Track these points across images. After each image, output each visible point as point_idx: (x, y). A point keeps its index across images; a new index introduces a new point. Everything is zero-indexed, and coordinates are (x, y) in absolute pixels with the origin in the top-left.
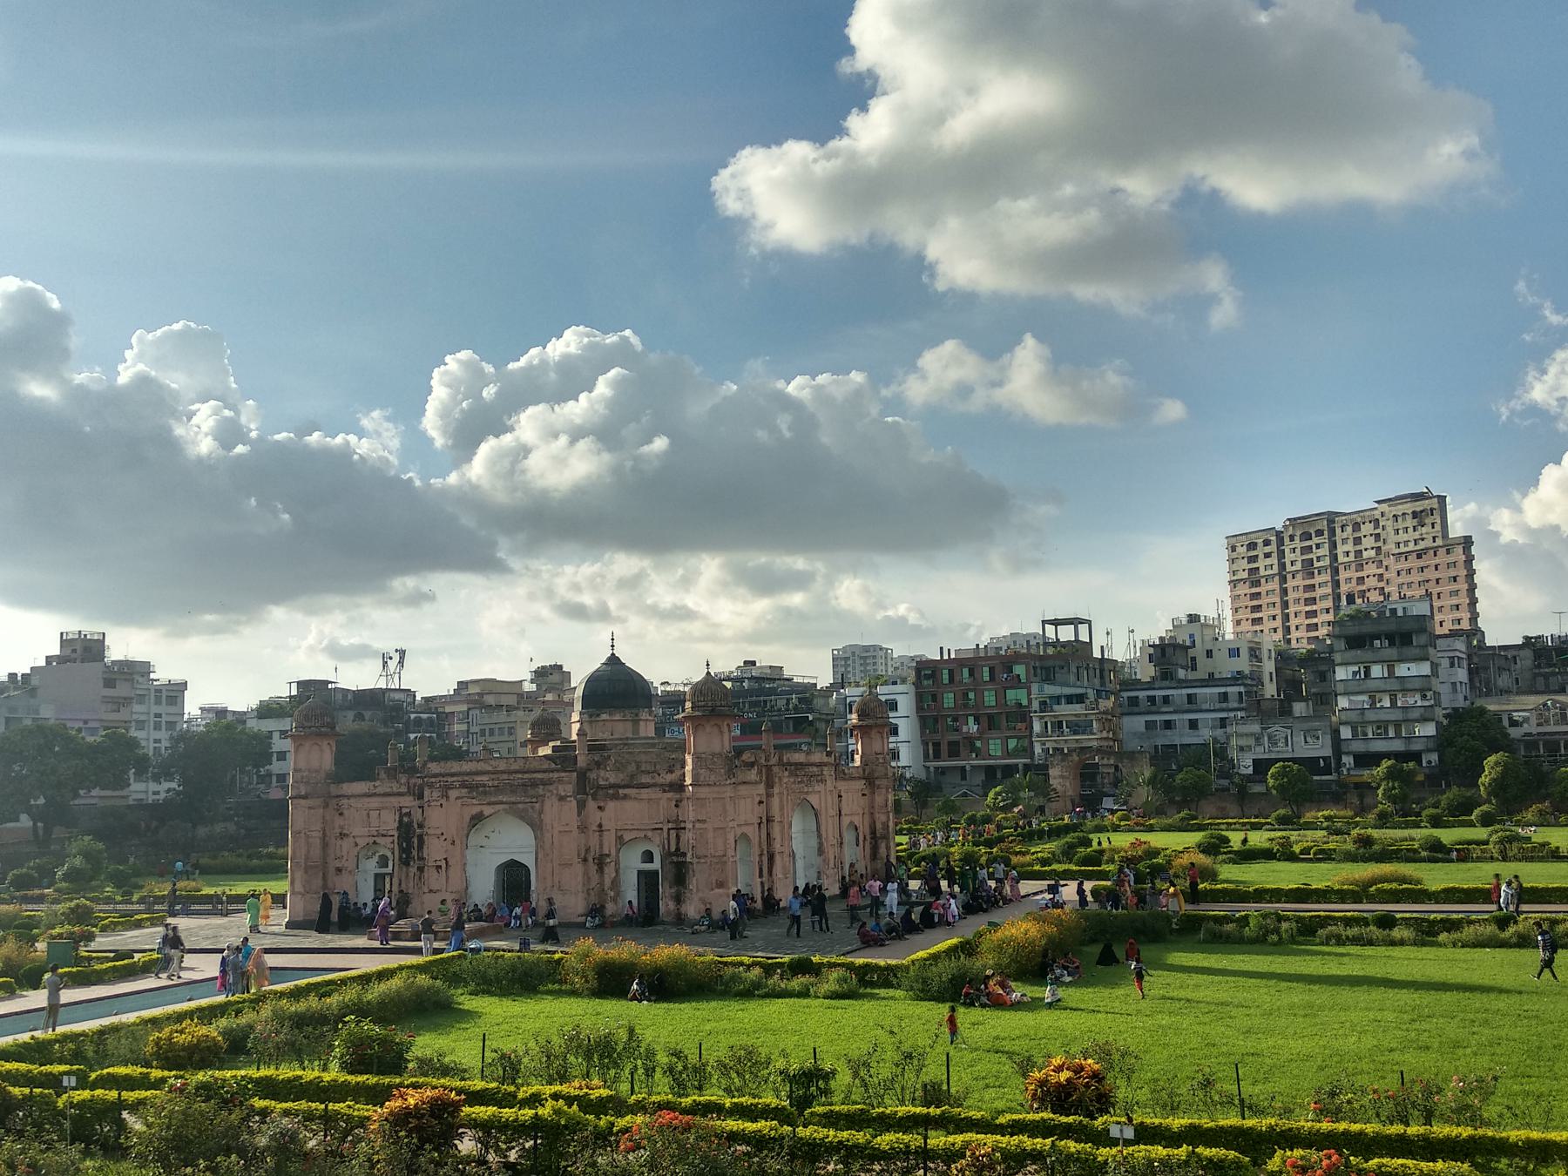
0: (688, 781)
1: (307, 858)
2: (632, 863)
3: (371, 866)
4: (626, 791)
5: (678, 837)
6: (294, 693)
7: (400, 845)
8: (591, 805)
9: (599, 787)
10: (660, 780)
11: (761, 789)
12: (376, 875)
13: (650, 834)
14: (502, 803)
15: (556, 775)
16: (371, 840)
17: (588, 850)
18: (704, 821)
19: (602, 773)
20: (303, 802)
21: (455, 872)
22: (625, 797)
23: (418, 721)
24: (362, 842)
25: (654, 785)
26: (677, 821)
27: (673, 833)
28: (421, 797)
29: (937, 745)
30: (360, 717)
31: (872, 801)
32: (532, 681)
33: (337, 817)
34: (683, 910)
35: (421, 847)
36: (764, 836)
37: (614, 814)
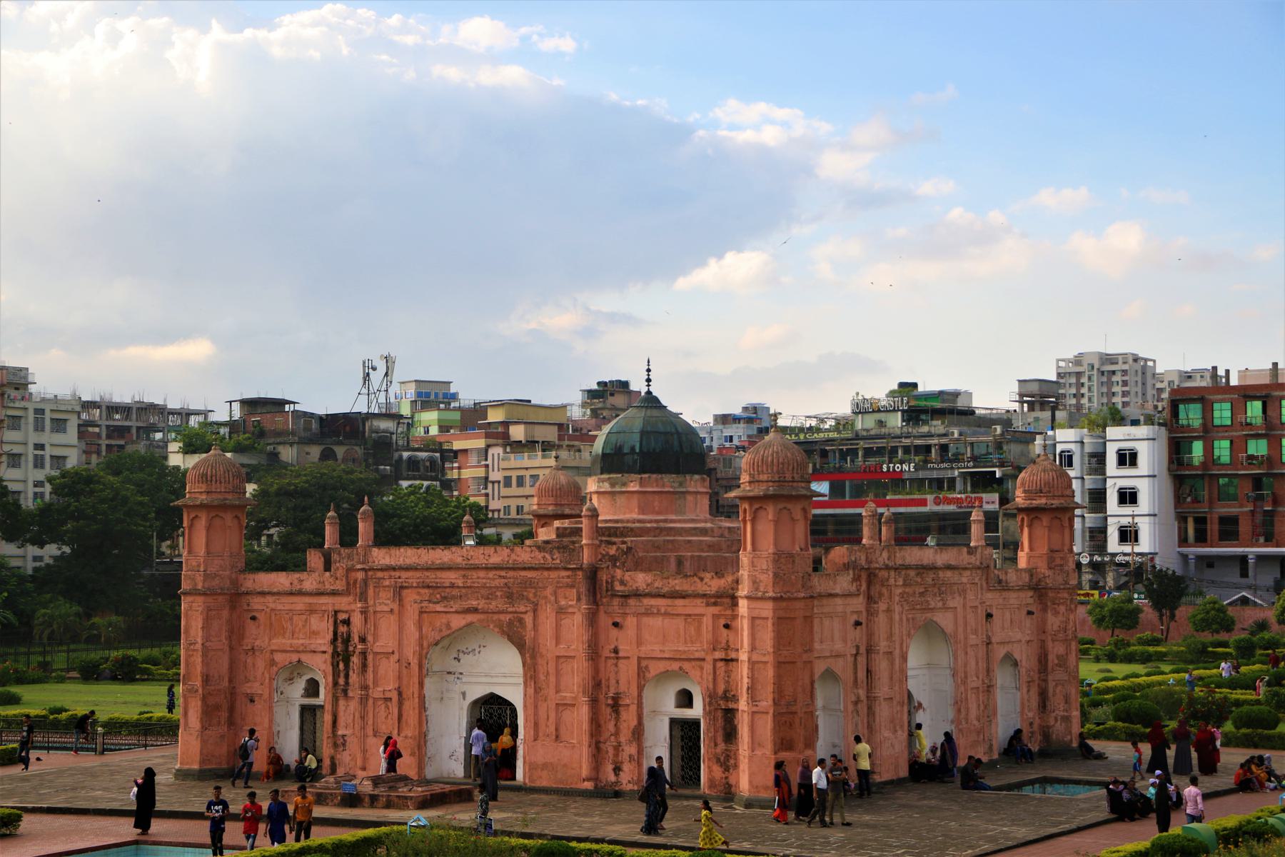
0: (743, 591)
1: (206, 679)
2: (662, 708)
6: (237, 415)
7: (335, 666)
10: (701, 588)
11: (859, 603)
13: (686, 666)
14: (476, 610)
16: (295, 658)
19: (619, 573)
23: (413, 463)
25: (696, 596)
28: (363, 597)
29: (1201, 521)
30: (327, 455)
31: (1044, 622)
32: (584, 405)
35: (364, 666)
36: (862, 675)
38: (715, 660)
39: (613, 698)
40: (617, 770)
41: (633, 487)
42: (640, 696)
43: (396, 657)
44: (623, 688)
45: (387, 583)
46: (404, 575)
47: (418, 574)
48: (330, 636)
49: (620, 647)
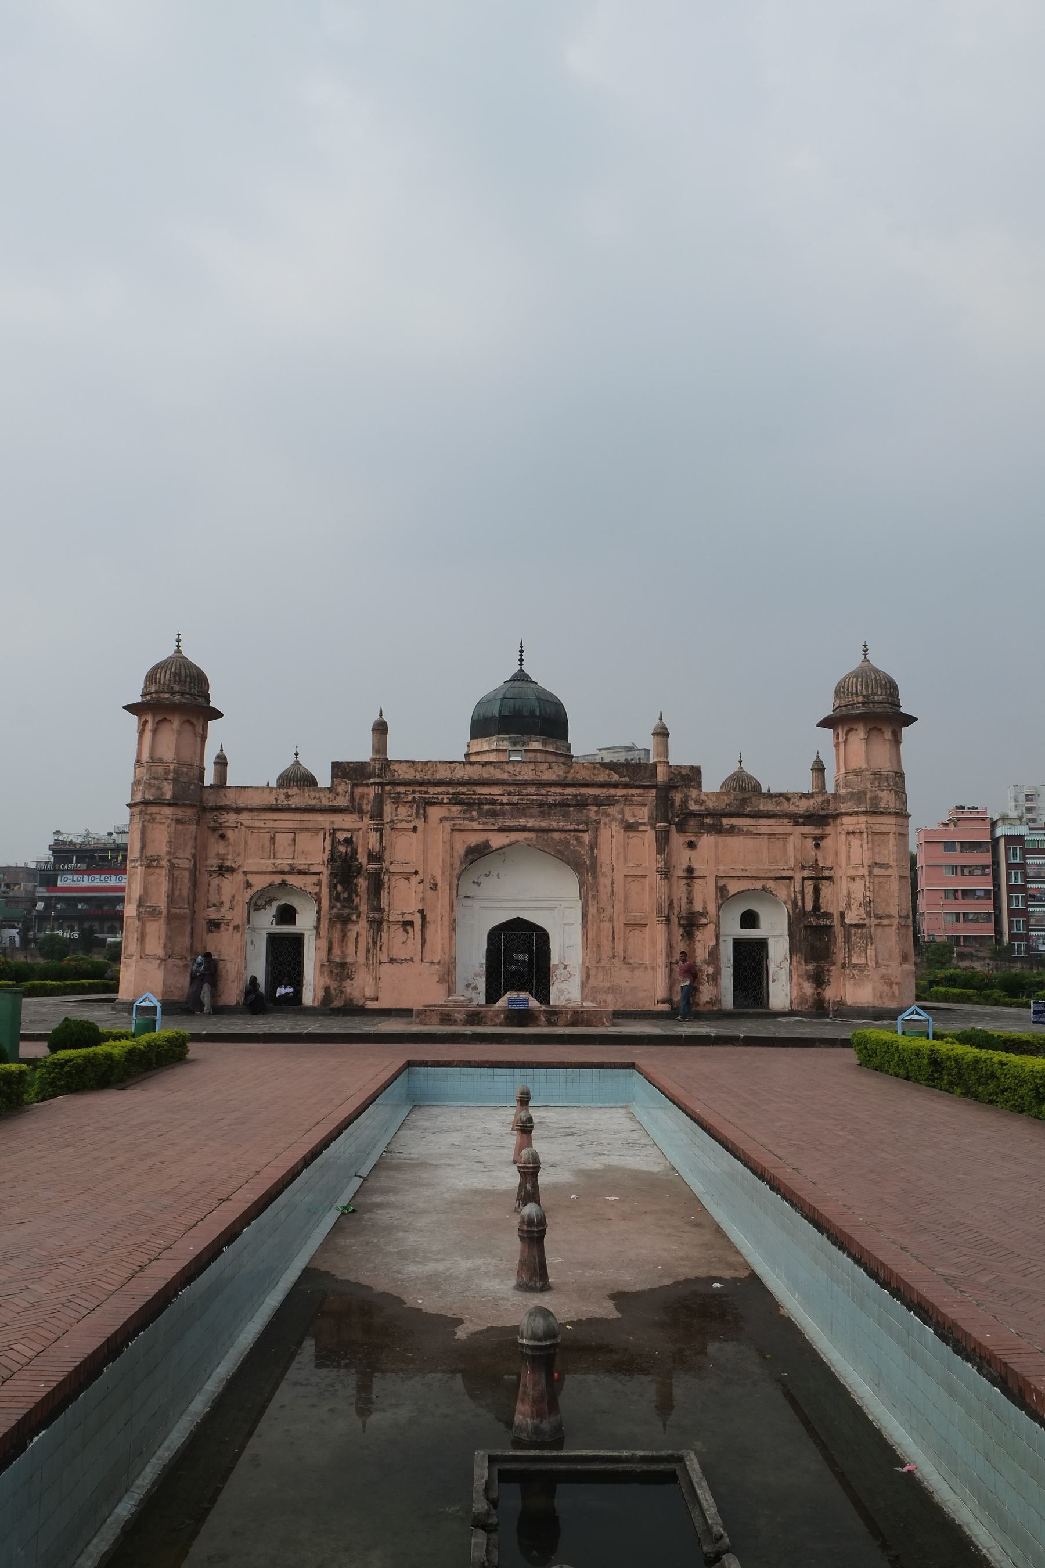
3: (266, 921)
4: (734, 821)
5: (817, 891)
7: (332, 887)
8: (677, 840)
9: (693, 814)
12: (274, 941)
13: (771, 885)
14: (524, 829)
15: (620, 792)
16: (277, 879)
17: (671, 904)
18: (887, 866)
19: (694, 793)
20: (167, 811)
21: (437, 934)
22: (732, 830)
24: (260, 882)
26: (815, 866)
27: (809, 886)
28: (378, 814)
33: (213, 839)
34: (830, 993)
37: (711, 855)
38: (804, 879)
39: (687, 918)
40: (691, 991)
41: (536, 745)
42: (718, 916)
43: (419, 878)
44: (698, 907)
45: (410, 798)
46: (432, 790)
47: (451, 790)
48: (326, 856)
49: (695, 866)
